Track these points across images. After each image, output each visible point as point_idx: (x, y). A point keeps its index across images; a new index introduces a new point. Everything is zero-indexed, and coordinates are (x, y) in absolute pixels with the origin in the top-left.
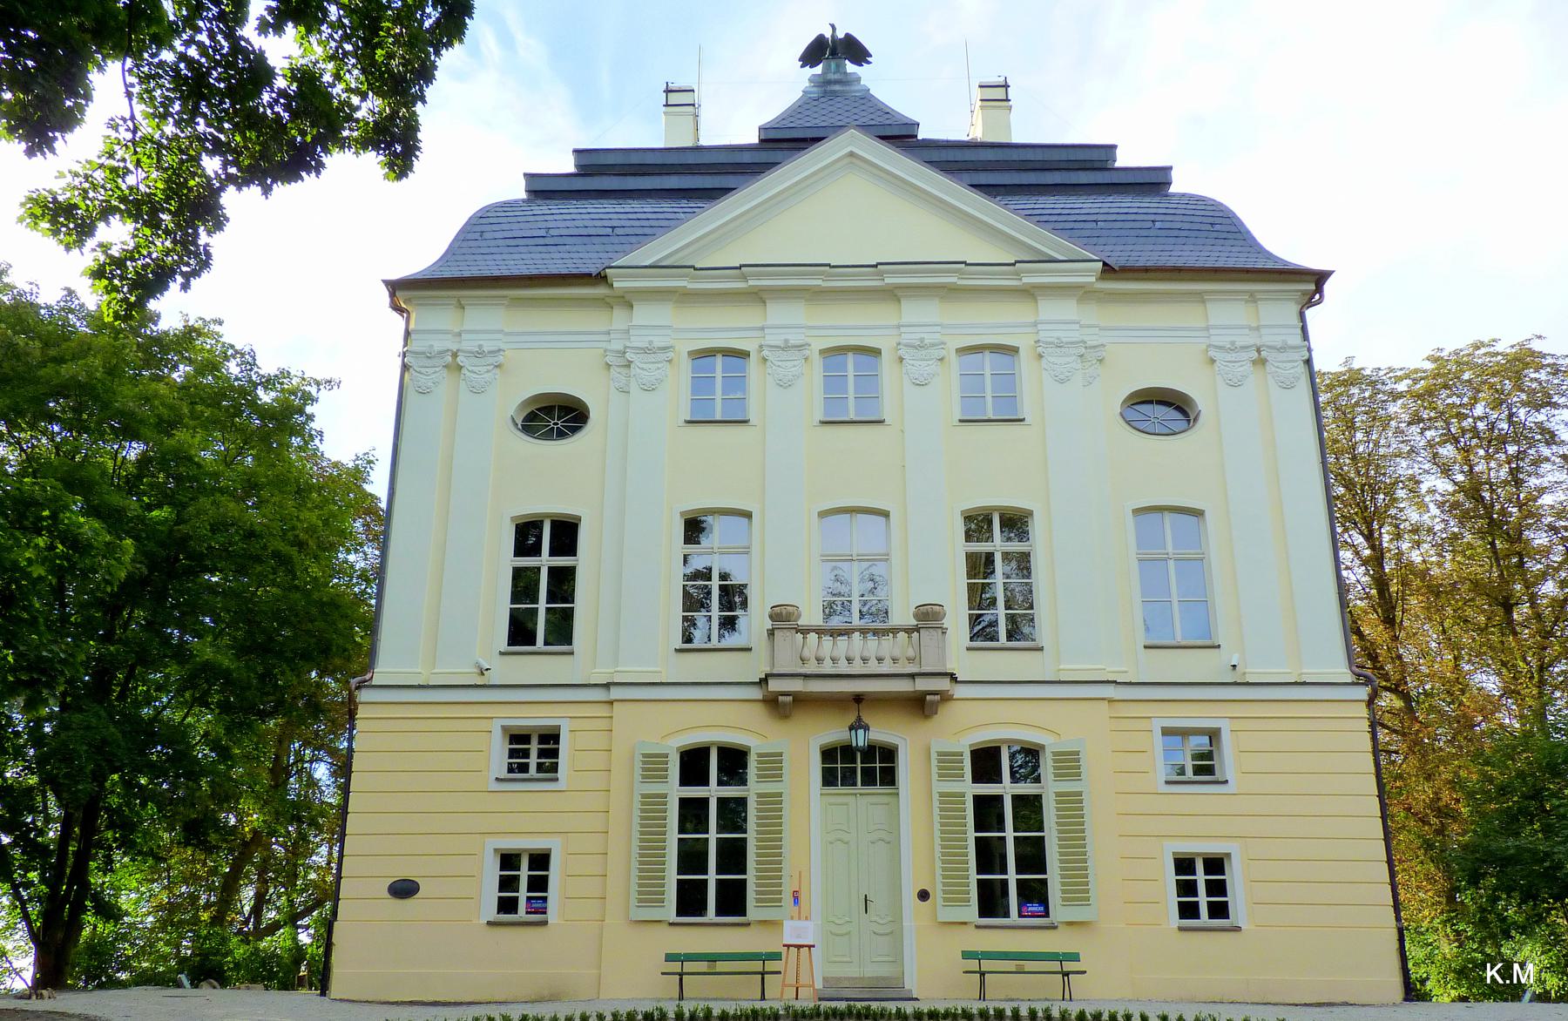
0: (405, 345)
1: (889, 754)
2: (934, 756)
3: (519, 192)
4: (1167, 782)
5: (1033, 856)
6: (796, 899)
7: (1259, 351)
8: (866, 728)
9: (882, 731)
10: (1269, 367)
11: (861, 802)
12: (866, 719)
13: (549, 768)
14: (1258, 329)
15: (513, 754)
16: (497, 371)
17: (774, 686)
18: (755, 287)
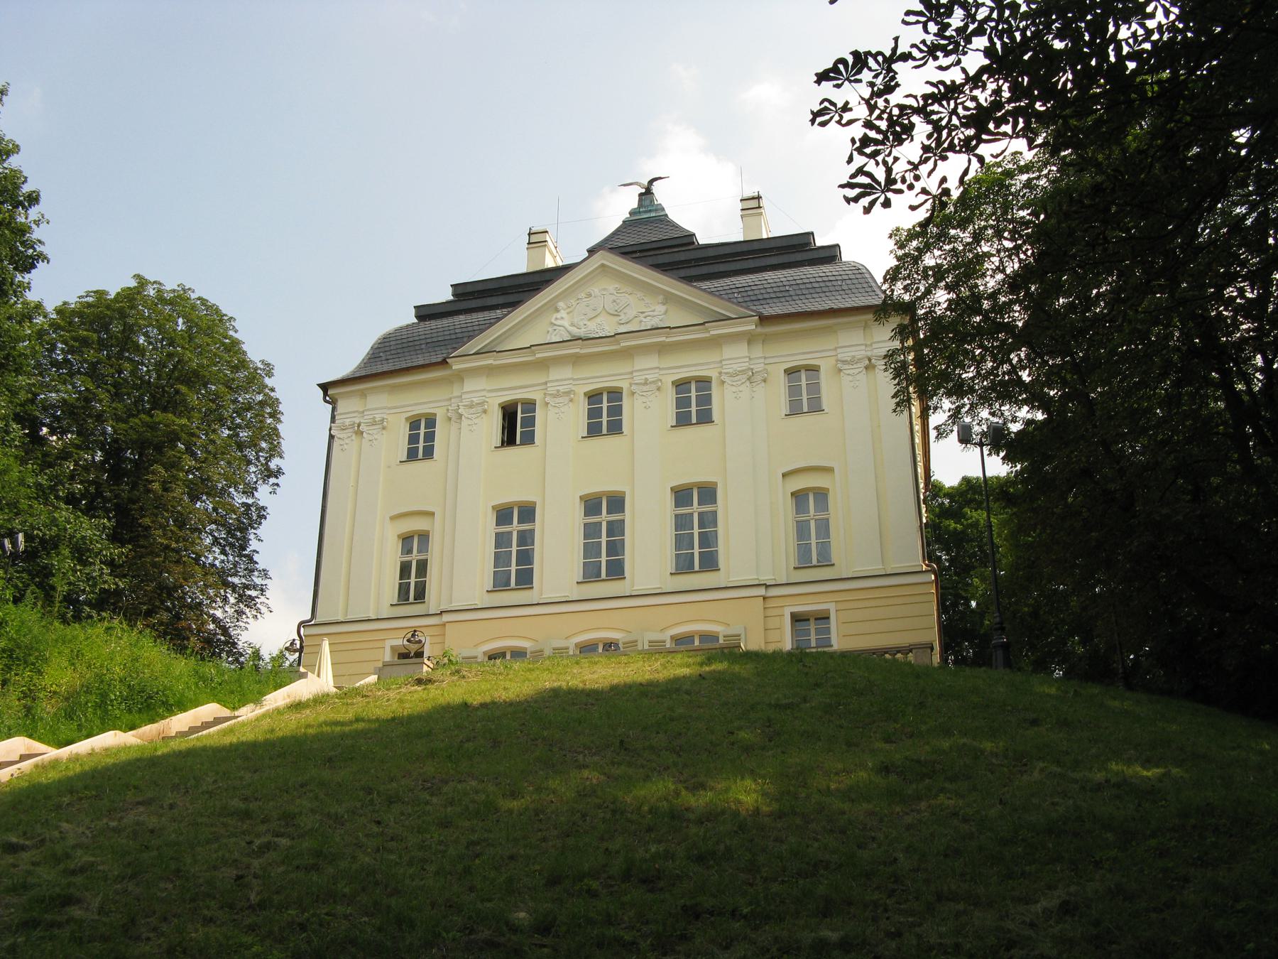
7: (870, 360)
18: (540, 360)
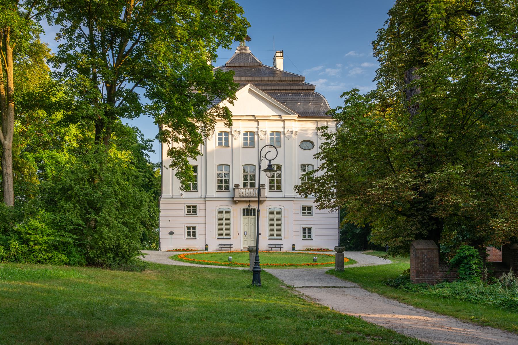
9: (254, 206)
11: (251, 220)
12: (251, 205)
13: (195, 212)
15: (188, 210)
17: (235, 199)
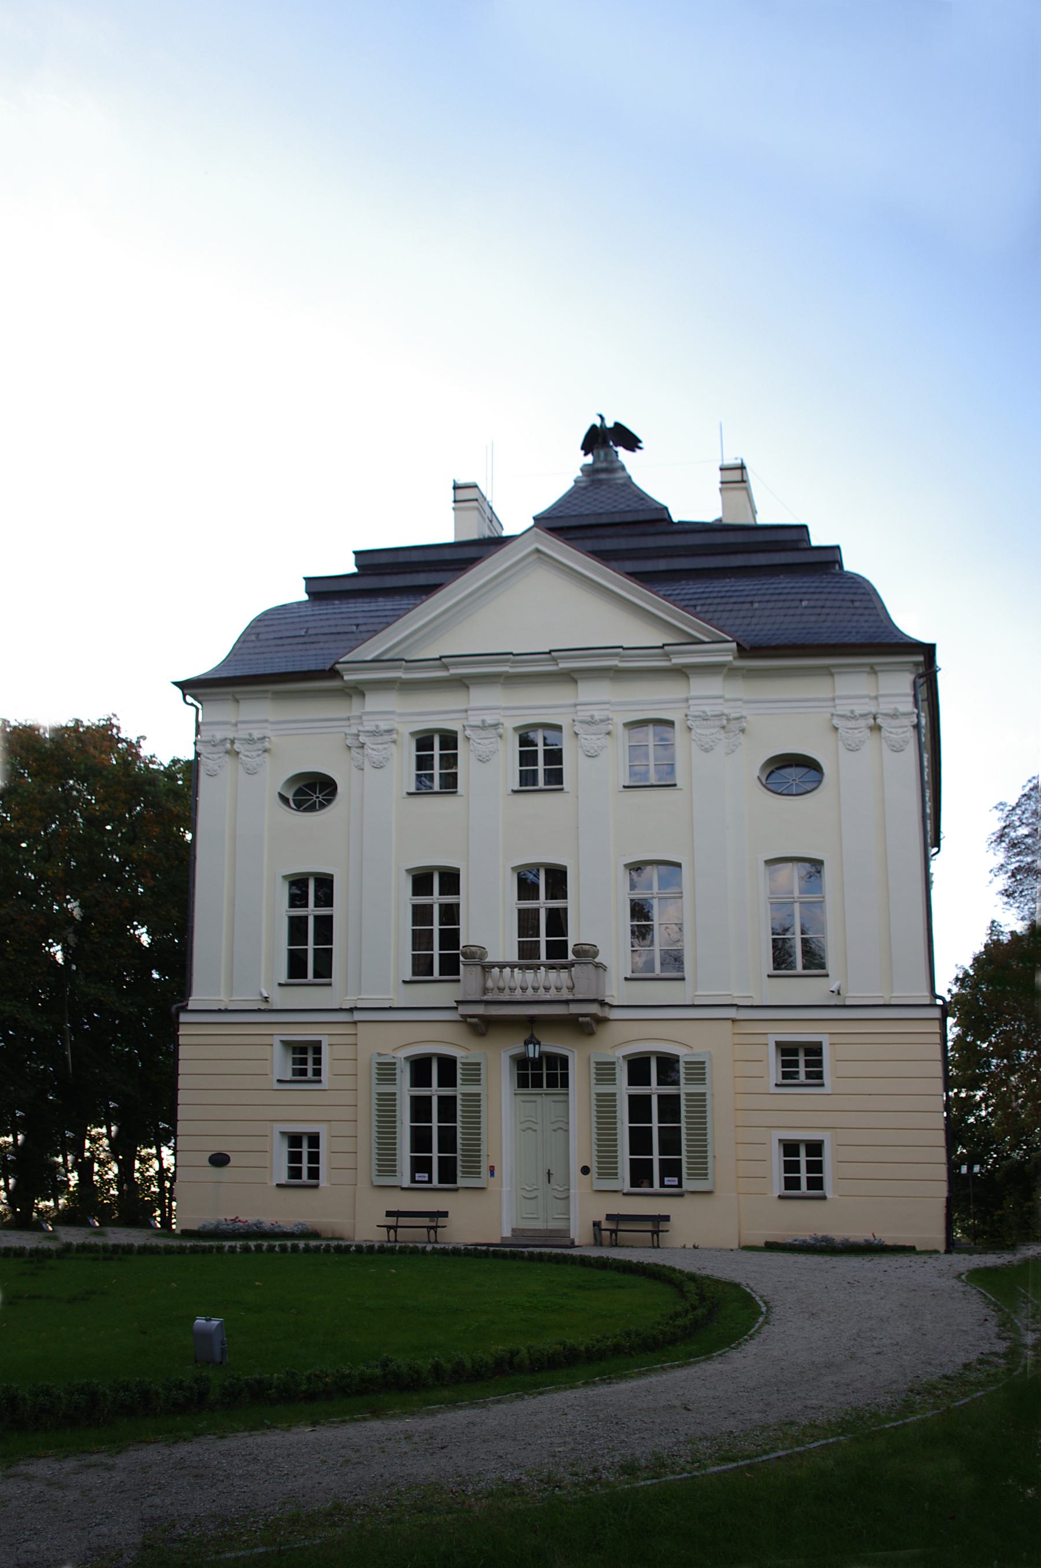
0: (197, 734)
1: (564, 1061)
2: (593, 1065)
3: (301, 595)
4: (777, 1085)
5: (671, 1142)
6: (492, 1174)
8: (539, 1043)
9: (552, 1045)
10: (884, 733)
12: (538, 1036)
14: (876, 698)
16: (266, 755)
